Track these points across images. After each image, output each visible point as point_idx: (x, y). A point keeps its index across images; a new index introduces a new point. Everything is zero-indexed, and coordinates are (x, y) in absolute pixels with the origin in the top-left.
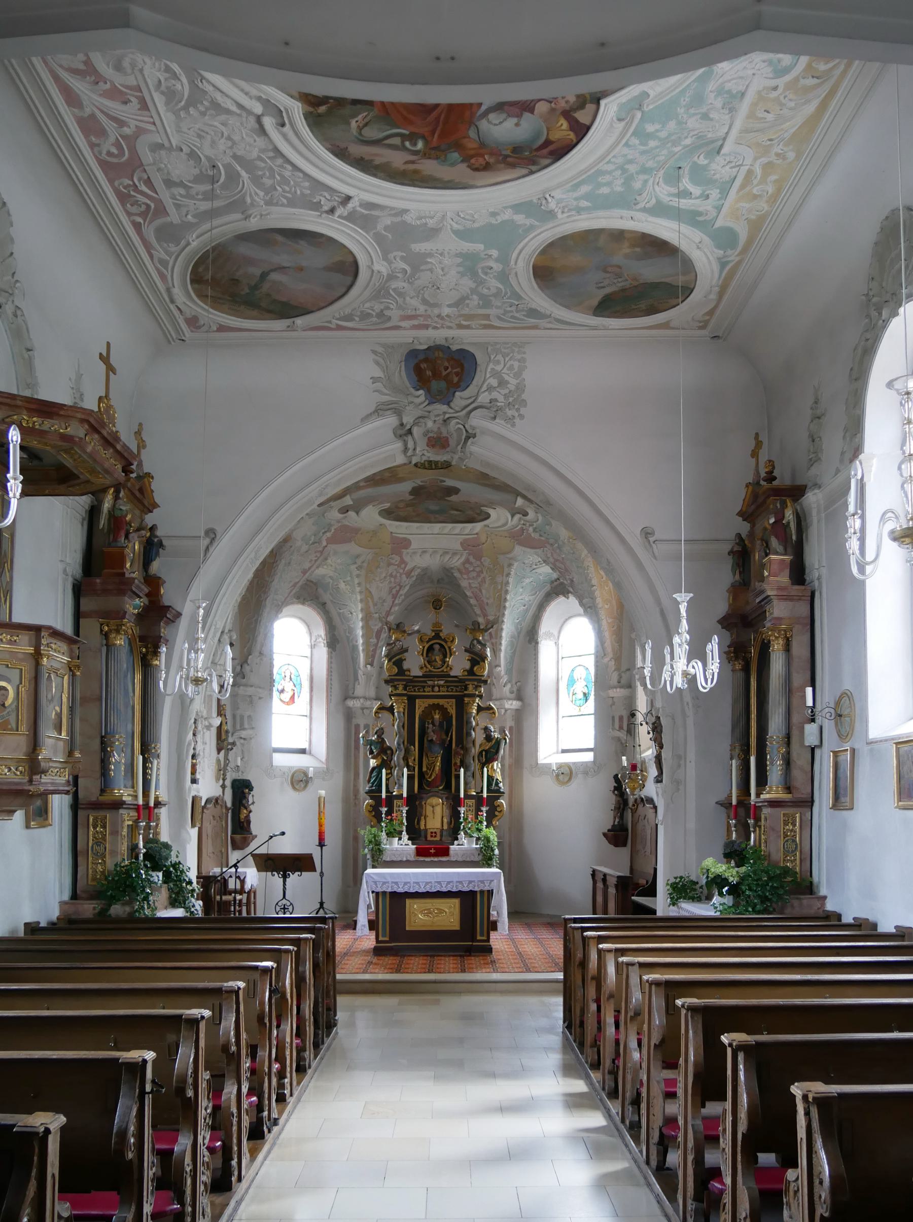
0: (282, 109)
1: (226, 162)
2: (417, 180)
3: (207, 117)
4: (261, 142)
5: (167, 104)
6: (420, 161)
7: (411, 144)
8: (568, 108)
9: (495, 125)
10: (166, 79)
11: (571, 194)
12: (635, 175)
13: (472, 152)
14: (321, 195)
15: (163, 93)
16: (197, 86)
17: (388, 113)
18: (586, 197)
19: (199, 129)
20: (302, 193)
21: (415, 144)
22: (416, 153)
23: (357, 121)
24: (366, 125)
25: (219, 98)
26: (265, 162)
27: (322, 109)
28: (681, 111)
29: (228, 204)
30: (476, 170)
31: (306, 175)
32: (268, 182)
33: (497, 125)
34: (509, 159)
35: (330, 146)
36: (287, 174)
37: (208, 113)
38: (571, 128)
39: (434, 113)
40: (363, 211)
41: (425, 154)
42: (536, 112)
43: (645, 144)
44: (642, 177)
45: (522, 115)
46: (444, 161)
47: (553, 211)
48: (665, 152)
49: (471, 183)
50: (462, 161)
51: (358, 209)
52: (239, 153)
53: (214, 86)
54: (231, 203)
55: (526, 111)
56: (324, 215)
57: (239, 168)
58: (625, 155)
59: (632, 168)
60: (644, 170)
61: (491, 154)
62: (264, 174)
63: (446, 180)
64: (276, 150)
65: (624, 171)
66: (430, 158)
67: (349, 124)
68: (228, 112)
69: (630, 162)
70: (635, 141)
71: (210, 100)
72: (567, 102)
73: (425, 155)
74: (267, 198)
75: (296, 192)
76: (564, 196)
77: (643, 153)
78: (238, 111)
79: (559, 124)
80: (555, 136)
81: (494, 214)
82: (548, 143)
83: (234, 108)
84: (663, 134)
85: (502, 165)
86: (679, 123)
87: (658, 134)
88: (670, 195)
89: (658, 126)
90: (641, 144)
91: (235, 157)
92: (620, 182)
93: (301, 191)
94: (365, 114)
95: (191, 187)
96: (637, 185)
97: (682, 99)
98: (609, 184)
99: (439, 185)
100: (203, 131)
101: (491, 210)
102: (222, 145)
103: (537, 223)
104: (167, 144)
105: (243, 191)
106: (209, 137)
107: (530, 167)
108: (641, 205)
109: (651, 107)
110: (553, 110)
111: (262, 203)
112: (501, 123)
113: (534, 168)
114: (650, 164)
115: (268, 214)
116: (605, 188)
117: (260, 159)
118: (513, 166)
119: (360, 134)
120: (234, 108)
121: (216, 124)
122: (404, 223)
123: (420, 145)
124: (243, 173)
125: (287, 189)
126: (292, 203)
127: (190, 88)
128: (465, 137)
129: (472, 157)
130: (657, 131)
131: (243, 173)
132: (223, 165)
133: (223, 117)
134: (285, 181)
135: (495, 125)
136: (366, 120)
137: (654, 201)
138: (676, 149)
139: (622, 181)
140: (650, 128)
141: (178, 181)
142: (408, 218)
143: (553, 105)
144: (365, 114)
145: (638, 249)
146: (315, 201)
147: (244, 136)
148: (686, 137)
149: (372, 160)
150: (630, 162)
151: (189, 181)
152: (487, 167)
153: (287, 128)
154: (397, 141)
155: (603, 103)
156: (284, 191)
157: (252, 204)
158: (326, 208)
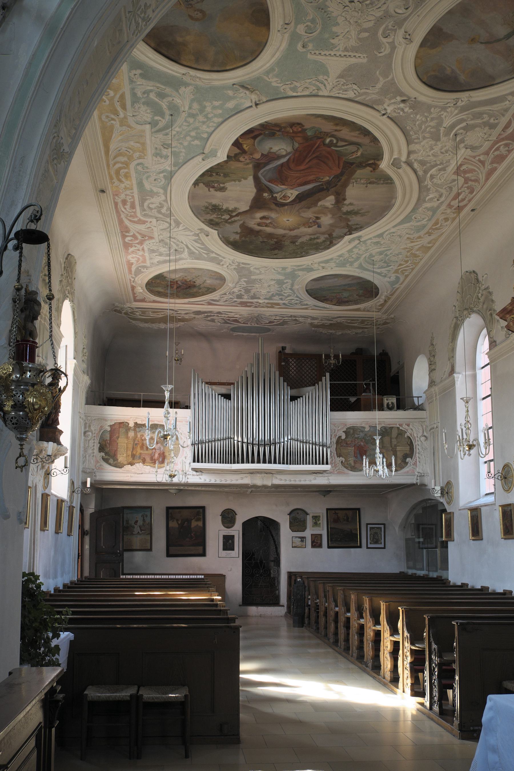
8: (243, 155)
9: (283, 149)
13: (299, 135)
17: (339, 158)
21: (331, 141)
22: (333, 136)
30: (299, 124)
34: (278, 129)
35: (379, 144)
38: (241, 145)
41: (327, 135)
42: (260, 154)
44: (194, 112)
45: (268, 153)
50: (306, 130)
61: (288, 132)
63: (320, 118)
66: (325, 133)
67: (362, 154)
69: (204, 123)
73: (327, 134)
80: (250, 141)
82: (255, 138)
84: (188, 138)
85: (282, 125)
92: (208, 109)
98: (214, 108)
112: (280, 150)
114: (191, 120)
116: (217, 105)
118: (276, 125)
123: (328, 140)
128: (301, 143)
129: (300, 132)
135: (283, 149)
136: (352, 155)
138: (177, 129)
145: (179, 39)
149: (360, 134)
152: (292, 125)
154: (340, 143)
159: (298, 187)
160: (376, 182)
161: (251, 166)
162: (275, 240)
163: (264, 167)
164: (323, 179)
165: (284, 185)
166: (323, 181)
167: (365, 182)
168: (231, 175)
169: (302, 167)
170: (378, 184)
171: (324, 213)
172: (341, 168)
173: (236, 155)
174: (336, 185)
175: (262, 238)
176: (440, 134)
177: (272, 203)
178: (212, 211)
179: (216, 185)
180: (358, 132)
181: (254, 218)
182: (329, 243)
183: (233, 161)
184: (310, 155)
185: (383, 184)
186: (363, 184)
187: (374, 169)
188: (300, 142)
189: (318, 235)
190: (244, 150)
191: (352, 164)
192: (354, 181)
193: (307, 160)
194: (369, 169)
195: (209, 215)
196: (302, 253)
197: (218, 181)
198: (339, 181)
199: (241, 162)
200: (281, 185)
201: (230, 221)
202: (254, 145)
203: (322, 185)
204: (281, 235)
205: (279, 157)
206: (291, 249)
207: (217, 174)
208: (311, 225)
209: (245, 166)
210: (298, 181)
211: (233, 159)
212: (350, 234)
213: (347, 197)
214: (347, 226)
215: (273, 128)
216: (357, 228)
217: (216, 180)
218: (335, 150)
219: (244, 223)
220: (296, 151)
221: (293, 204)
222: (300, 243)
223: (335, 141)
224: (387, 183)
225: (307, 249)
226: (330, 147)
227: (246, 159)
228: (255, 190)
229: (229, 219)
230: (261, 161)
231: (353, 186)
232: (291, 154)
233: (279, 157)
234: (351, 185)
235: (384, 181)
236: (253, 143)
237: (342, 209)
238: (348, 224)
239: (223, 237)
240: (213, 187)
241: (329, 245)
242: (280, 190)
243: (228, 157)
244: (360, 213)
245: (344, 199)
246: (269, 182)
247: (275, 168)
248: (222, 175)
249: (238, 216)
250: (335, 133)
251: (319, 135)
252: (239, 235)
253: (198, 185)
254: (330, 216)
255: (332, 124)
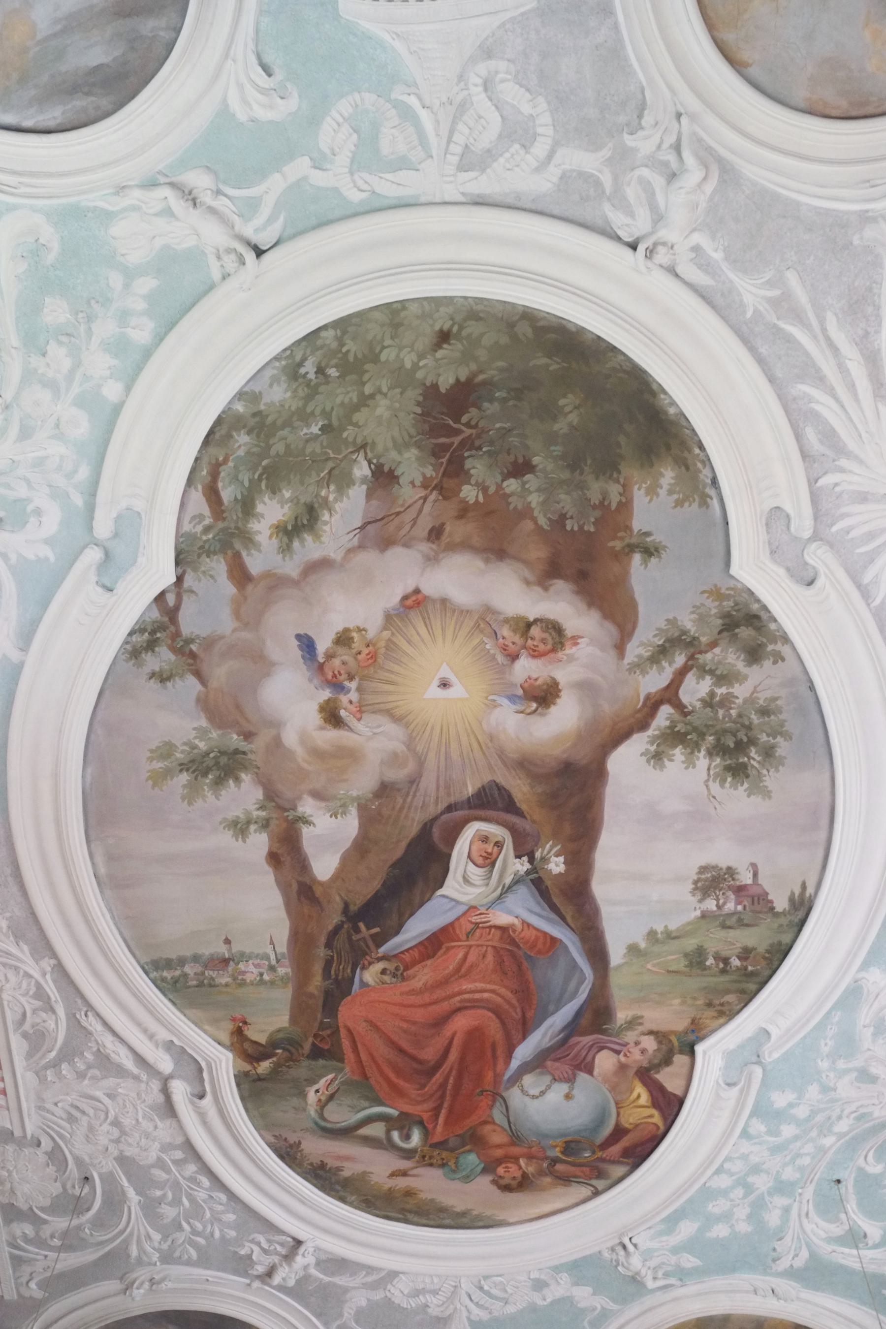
0: (203, 1064)
1: (104, 1170)
2: (410, 1212)
3: (86, 1082)
4: (164, 1131)
5: (29, 1055)
6: (415, 1172)
7: (401, 1137)
8: (645, 1064)
9: (534, 1097)
10: (34, 1011)
11: (664, 1238)
12: (767, 1198)
13: (499, 1153)
14: (253, 1241)
15: (25, 1035)
16: (79, 1022)
18: (689, 1246)
19: (72, 1105)
20: (223, 1238)
21: (407, 1137)
22: (408, 1154)
23: (317, 1091)
24: (331, 1098)
25: (108, 1042)
26: (168, 1171)
27: (265, 1066)
28: (824, 1065)
29: (100, 1259)
30: (507, 1188)
31: (232, 1196)
32: (169, 1212)
33: (537, 1097)
34: (559, 1167)
35: (273, 1140)
36: (201, 1195)
37: (89, 1075)
38: (655, 1104)
39: (438, 1075)
40: (321, 1276)
41: (424, 1157)
42: (596, 1072)
43: (777, 1133)
44: (780, 1201)
45: (575, 1076)
46: (454, 1171)
47: (638, 1273)
48: (809, 1148)
49: (501, 1216)
50: (485, 1171)
51: (313, 1271)
52: (129, 1152)
53: (105, 1024)
54: (108, 1254)
55: (580, 1070)
56: (257, 1284)
57: (125, 1183)
58: (744, 1157)
59: (762, 1183)
60: (782, 1188)
61: (530, 1157)
62: (164, 1195)
63: (458, 1209)
64: (189, 1146)
65: (749, 1189)
66: (431, 1165)
67: (303, 1095)
68: (120, 1071)
69: (756, 1169)
70: (758, 1127)
71: (95, 1049)
72: (643, 1051)
73: (425, 1159)
74: (165, 1246)
75: (212, 1235)
76: (654, 1245)
77: (775, 1150)
78: (135, 1071)
79: (635, 1094)
80: (630, 1118)
81: (539, 1285)
82: (619, 1132)
83: (129, 1063)
84: (801, 1112)
85: (548, 1180)
86: (826, 1089)
87: (793, 1111)
88: (830, 1240)
89: (791, 1096)
90: (769, 1132)
91: (122, 1160)
92: (742, 1212)
93: (221, 1231)
94: (331, 1076)
95: (45, 1222)
96: (773, 1219)
97: (822, 1043)
99: (447, 1222)
100: (77, 1108)
101: (535, 1275)
102: (105, 1133)
103: (612, 1306)
104: (18, 1133)
105: (128, 1230)
106: (84, 1120)
107: (594, 1182)
108: (783, 1264)
109: (776, 1055)
110: (622, 1068)
111: (155, 1257)
112: (543, 1093)
113: (600, 1184)
114: (789, 1174)
115: (163, 1279)
116: (720, 1226)
117: (160, 1164)
118: (566, 1180)
119: (322, 1116)
120: (129, 1063)
121: (99, 1094)
122: (388, 1302)
123: (416, 1138)
124: (131, 1193)
125: (199, 1226)
126: (204, 1261)
127: (68, 1026)
128: (485, 1123)
129: (499, 1162)
130: (791, 1105)
131: (131, 1193)
132: (101, 1176)
133: (111, 1082)
134: (196, 1211)
135: (534, 1097)
136: (331, 1090)
137: (805, 1254)
138: (828, 1141)
139: (748, 1210)
140: (780, 1100)
141: (25, 1207)
142: (398, 1292)
143: (622, 1057)
144: (331, 1076)
146: (243, 1252)
147: (140, 1120)
148: (840, 1118)
149: (339, 1169)
150: (756, 1169)
151: (42, 1209)
152: (523, 1184)
153: (208, 1101)
154: (376, 1130)
155: (699, 1049)
156: (194, 1232)
157: (140, 1262)
158: (260, 1269)
159: (452, 924)
160: (206, 967)
161: (621, 1016)
162: (469, 493)
163: (578, 1014)
164: (384, 972)
165: (503, 929)
166: (379, 959)
167: (242, 966)
168: (681, 965)
169: (461, 1023)
170: (196, 958)
171: (317, 754)
172: (343, 1033)
173: (667, 1061)
174: (329, 945)
175: (526, 513)
176: (129, 1180)
177: (524, 807)
178: (749, 728)
179: (730, 906)
180: (346, 1173)
181: (586, 688)
182: (227, 494)
183: (673, 1032)
184: (451, 1080)
185: (182, 962)
186: (244, 957)
187: (238, 1033)
188: (488, 1128)
189: (291, 568)
190: (645, 1084)
191: (316, 1053)
192: (281, 971)
193: (453, 1055)
194: (258, 1034)
195: (762, 698)
196: (320, 371)
197: (724, 927)
198: (328, 963)
199: (651, 1033)
200: (512, 926)
201: (680, 660)
202: (617, 1104)
203: (380, 940)
204: (453, 547)
205: (537, 1063)
206: (382, 407)
207: (726, 961)
208: (344, 655)
209: (639, 1013)
210: (461, 955)
211: (676, 1044)
212: (160, 598)
213: (268, 877)
214: (193, 655)
215: (572, 1169)
216: (151, 646)
217: (732, 934)
218: (382, 1104)
219: (620, 648)
220: (496, 1095)
221: (450, 808)
222: (351, 483)
223: (395, 1135)
224: (169, 964)
225: (305, 417)
226: (402, 1114)
227: (637, 1043)
228: (599, 889)
229: (681, 674)
230: (587, 1040)
231: (272, 943)
232: (506, 1077)
233: (537, 1063)
234: (282, 947)
235: (185, 975)
236: (622, 1111)
237: (258, 794)
238: (198, 674)
239: (704, 501)
240: (740, 890)
241: (215, 475)
242: (511, 900)
243: (692, 1053)
244: (184, 767)
245: (274, 858)
246: (554, 941)
247: (545, 1014)
248: (710, 961)
249: (648, 697)
250: (404, 1164)
251: (445, 1154)
252: (638, 523)
253: (792, 900)
254: (290, 738)
255: (423, 1196)
